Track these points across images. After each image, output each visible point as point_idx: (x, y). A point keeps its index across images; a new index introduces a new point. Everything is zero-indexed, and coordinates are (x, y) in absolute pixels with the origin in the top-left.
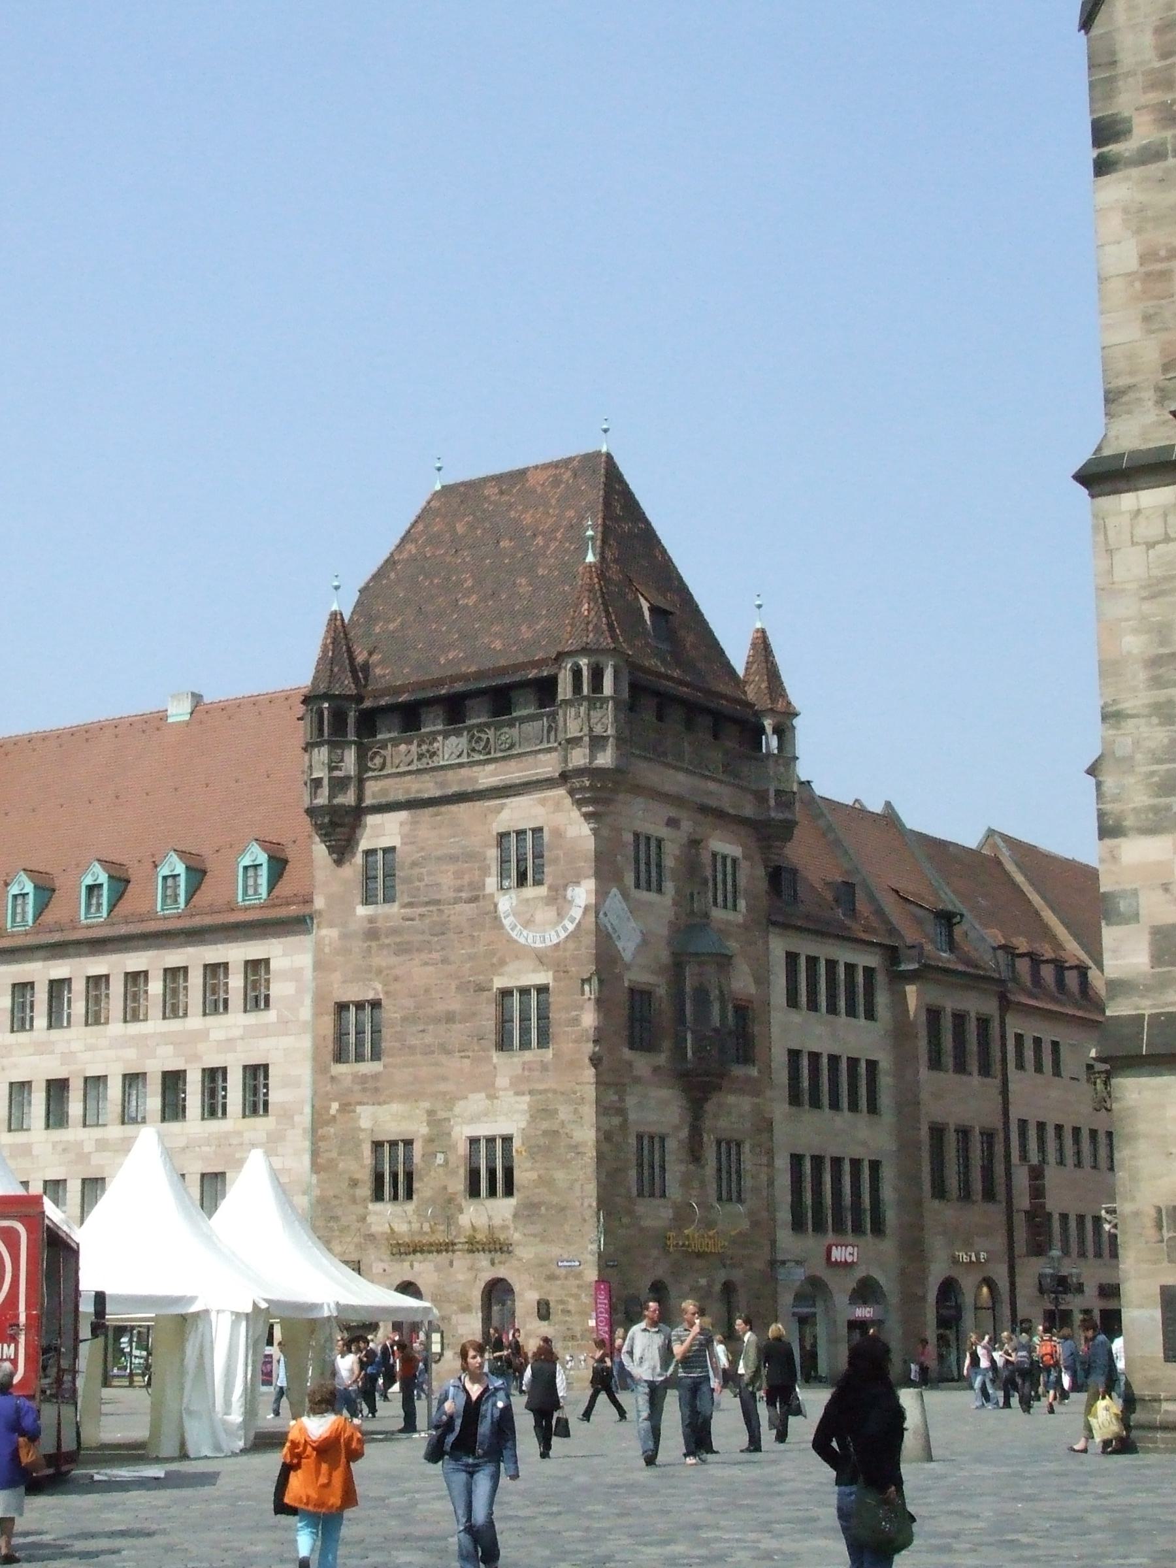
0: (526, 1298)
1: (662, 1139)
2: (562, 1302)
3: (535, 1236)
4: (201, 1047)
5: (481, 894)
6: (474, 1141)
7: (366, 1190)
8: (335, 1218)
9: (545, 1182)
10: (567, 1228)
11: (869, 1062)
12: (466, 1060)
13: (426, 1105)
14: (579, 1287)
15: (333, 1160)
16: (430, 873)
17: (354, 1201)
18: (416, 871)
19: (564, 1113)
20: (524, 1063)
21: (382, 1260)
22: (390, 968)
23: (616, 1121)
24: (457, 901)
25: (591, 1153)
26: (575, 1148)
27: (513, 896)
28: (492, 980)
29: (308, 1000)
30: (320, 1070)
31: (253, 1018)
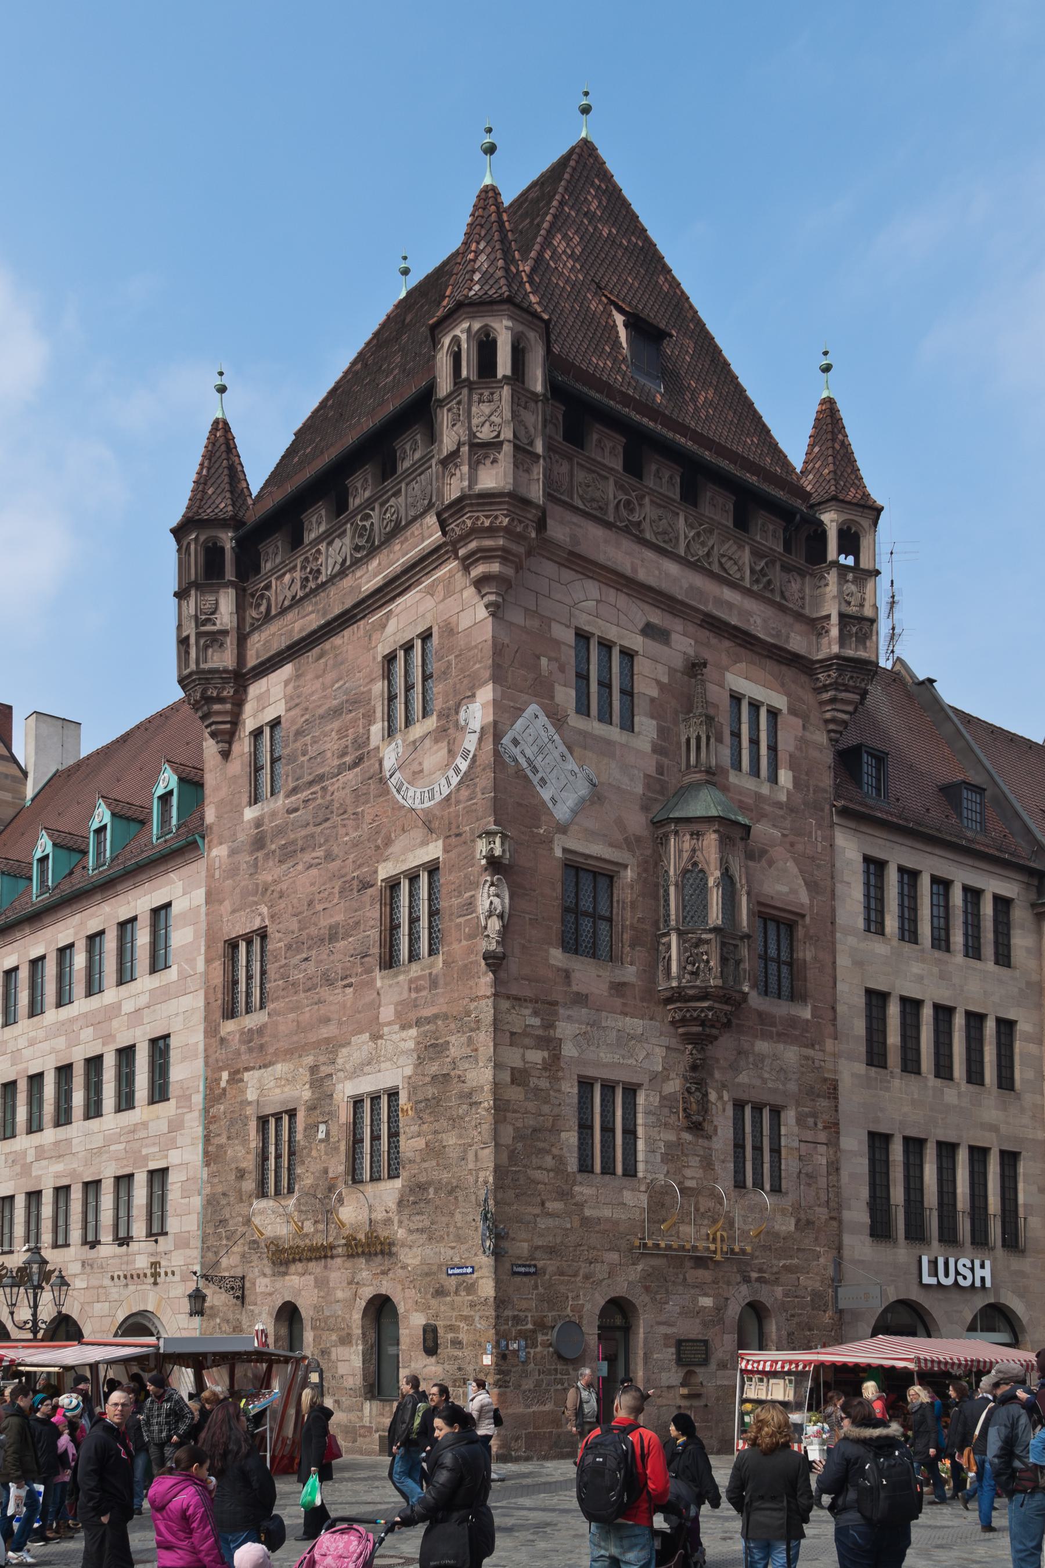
0: (412, 1322)
1: (631, 1091)
2: (451, 1328)
3: (421, 1231)
4: (115, 1023)
6: (357, 1102)
7: (249, 1185)
8: (223, 1222)
9: (434, 1151)
10: (458, 1217)
11: (999, 1021)
13: (309, 1060)
14: (472, 1305)
20: (411, 981)
21: (265, 1275)
22: (275, 882)
23: (536, 1056)
25: (487, 1101)
26: (469, 1098)
28: (376, 872)
30: (211, 1031)
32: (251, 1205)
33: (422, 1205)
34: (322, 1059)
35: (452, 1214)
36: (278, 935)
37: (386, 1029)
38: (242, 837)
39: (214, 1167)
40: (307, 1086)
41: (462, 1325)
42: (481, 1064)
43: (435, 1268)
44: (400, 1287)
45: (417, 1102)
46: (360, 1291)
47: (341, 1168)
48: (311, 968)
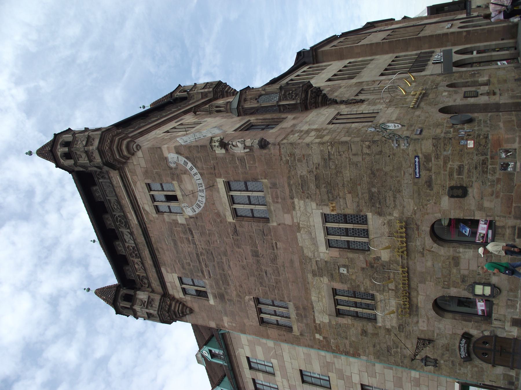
0: (447, 208)
2: (451, 175)
3: (395, 197)
5: (187, 227)
6: (329, 244)
7: (369, 327)
8: (389, 349)
10: (387, 169)
12: (278, 246)
13: (310, 276)
14: (437, 157)
15: (350, 344)
16: (185, 258)
17: (376, 335)
18: (187, 267)
19: (302, 170)
20: (273, 201)
21: (418, 322)
22: (236, 290)
24: (194, 243)
26: (327, 159)
27: (183, 205)
28: (230, 223)
29: (264, 341)
31: (278, 373)
32: (380, 327)
33: (381, 198)
34: (309, 267)
35: (386, 174)
36: (257, 291)
37: (295, 221)
38: (220, 307)
39: (361, 351)
40: (322, 279)
41: (449, 166)
42: (310, 153)
43: (416, 188)
44: (426, 216)
45: (329, 200)
46: (428, 247)
47: (361, 257)
48: (270, 270)
